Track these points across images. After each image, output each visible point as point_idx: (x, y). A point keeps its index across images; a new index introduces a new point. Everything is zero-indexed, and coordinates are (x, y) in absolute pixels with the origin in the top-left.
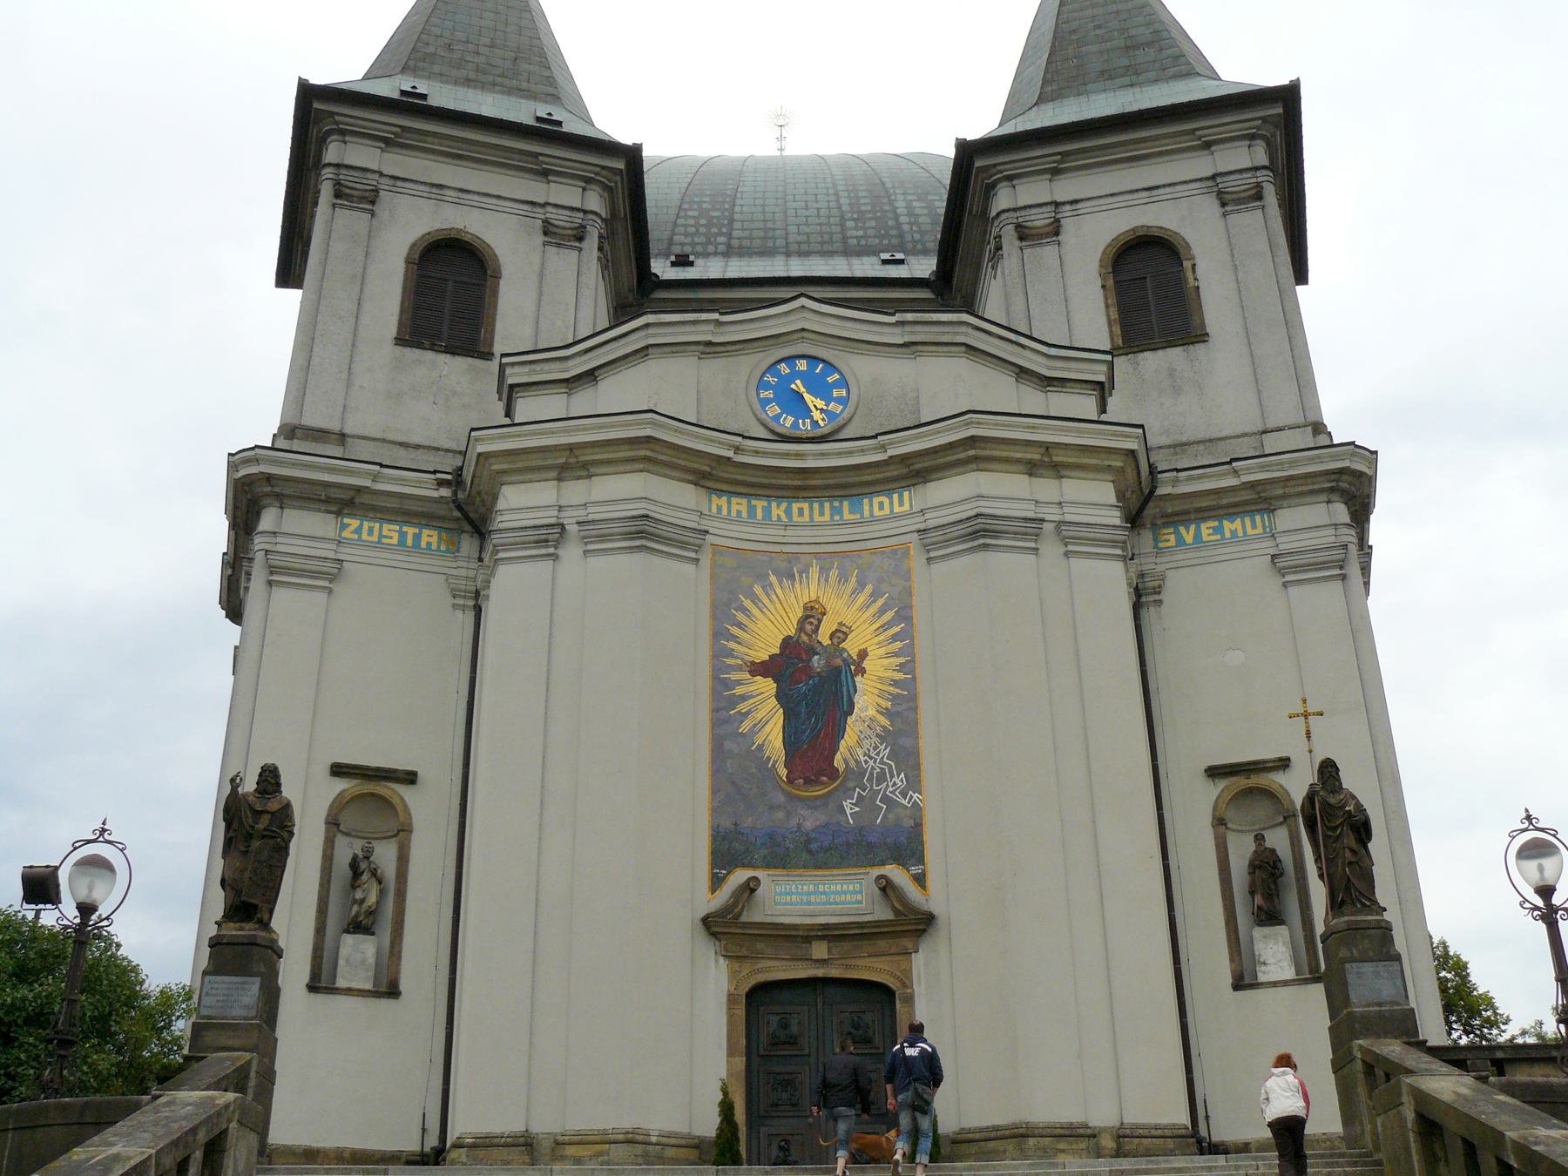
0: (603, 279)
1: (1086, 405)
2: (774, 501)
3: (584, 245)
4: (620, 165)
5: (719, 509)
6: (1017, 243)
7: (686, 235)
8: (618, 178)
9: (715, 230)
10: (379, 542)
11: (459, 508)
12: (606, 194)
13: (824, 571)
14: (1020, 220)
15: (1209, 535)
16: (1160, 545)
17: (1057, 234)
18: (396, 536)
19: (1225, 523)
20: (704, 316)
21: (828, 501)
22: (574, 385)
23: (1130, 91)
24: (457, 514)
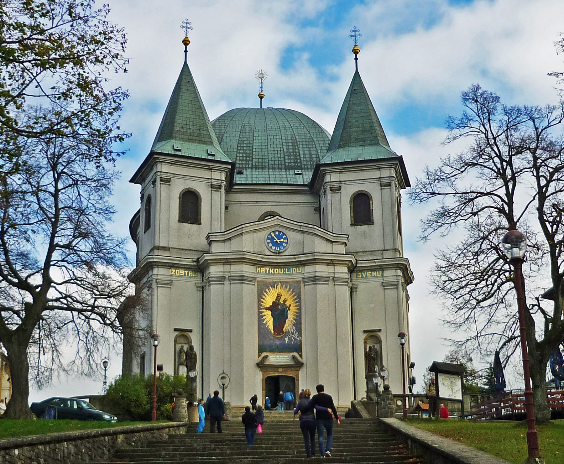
4: (230, 167)
7: (240, 160)
13: (282, 286)
19: (373, 273)
23: (361, 148)
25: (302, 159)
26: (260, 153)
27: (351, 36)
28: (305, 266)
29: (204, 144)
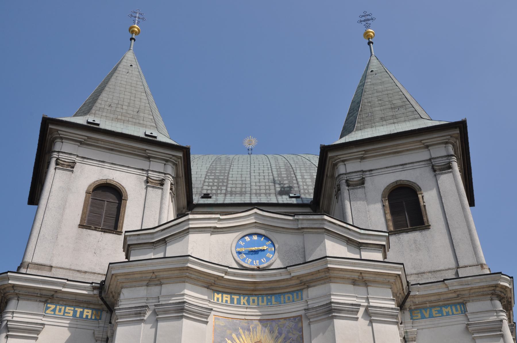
0: (172, 201)
1: (378, 256)
2: (242, 296)
3: (164, 187)
5: (218, 299)
6: (347, 188)
7: (208, 186)
8: (180, 160)
9: (221, 184)
10: (64, 315)
11: (102, 299)
12: (174, 167)
14: (348, 178)
15: (436, 314)
16: (414, 318)
17: (363, 183)
18: (72, 312)
19: (443, 308)
20: (213, 216)
21: (266, 296)
22: (157, 245)
23: (393, 125)
24: (101, 302)
25: (301, 183)
26: (240, 179)
27: (361, 21)
28: (308, 287)
29: (143, 127)
